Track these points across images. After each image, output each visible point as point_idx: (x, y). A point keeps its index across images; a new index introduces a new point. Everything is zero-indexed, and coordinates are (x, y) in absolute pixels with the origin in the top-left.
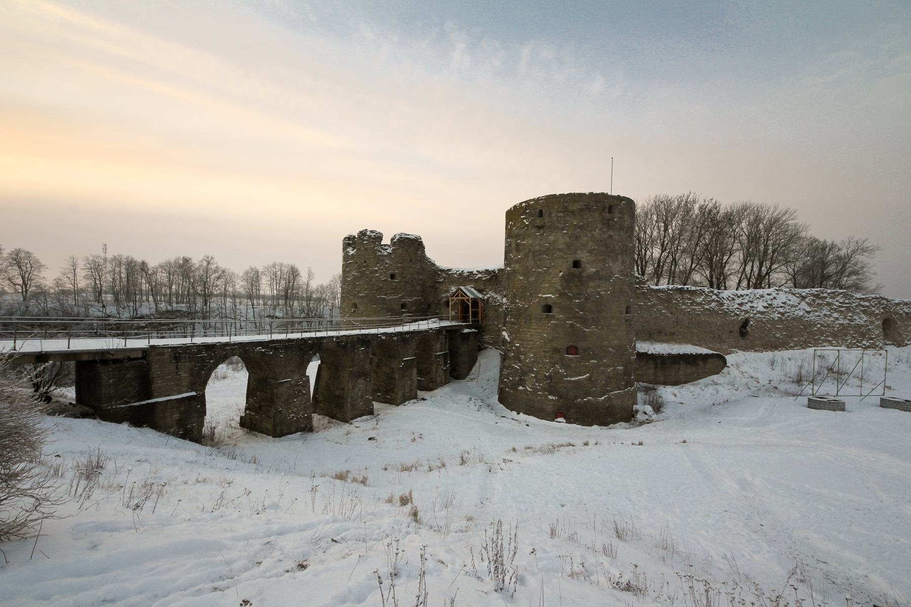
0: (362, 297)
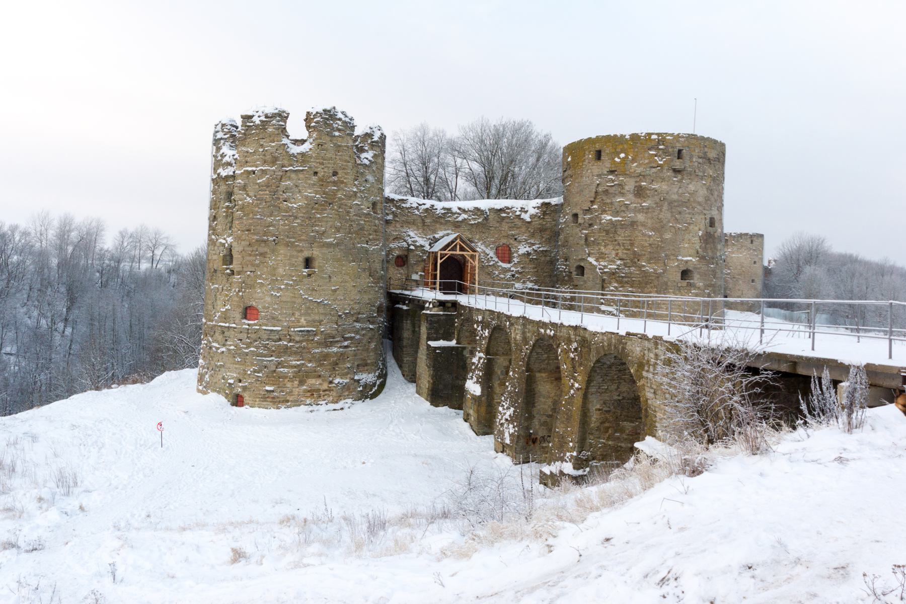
0: (329, 245)
